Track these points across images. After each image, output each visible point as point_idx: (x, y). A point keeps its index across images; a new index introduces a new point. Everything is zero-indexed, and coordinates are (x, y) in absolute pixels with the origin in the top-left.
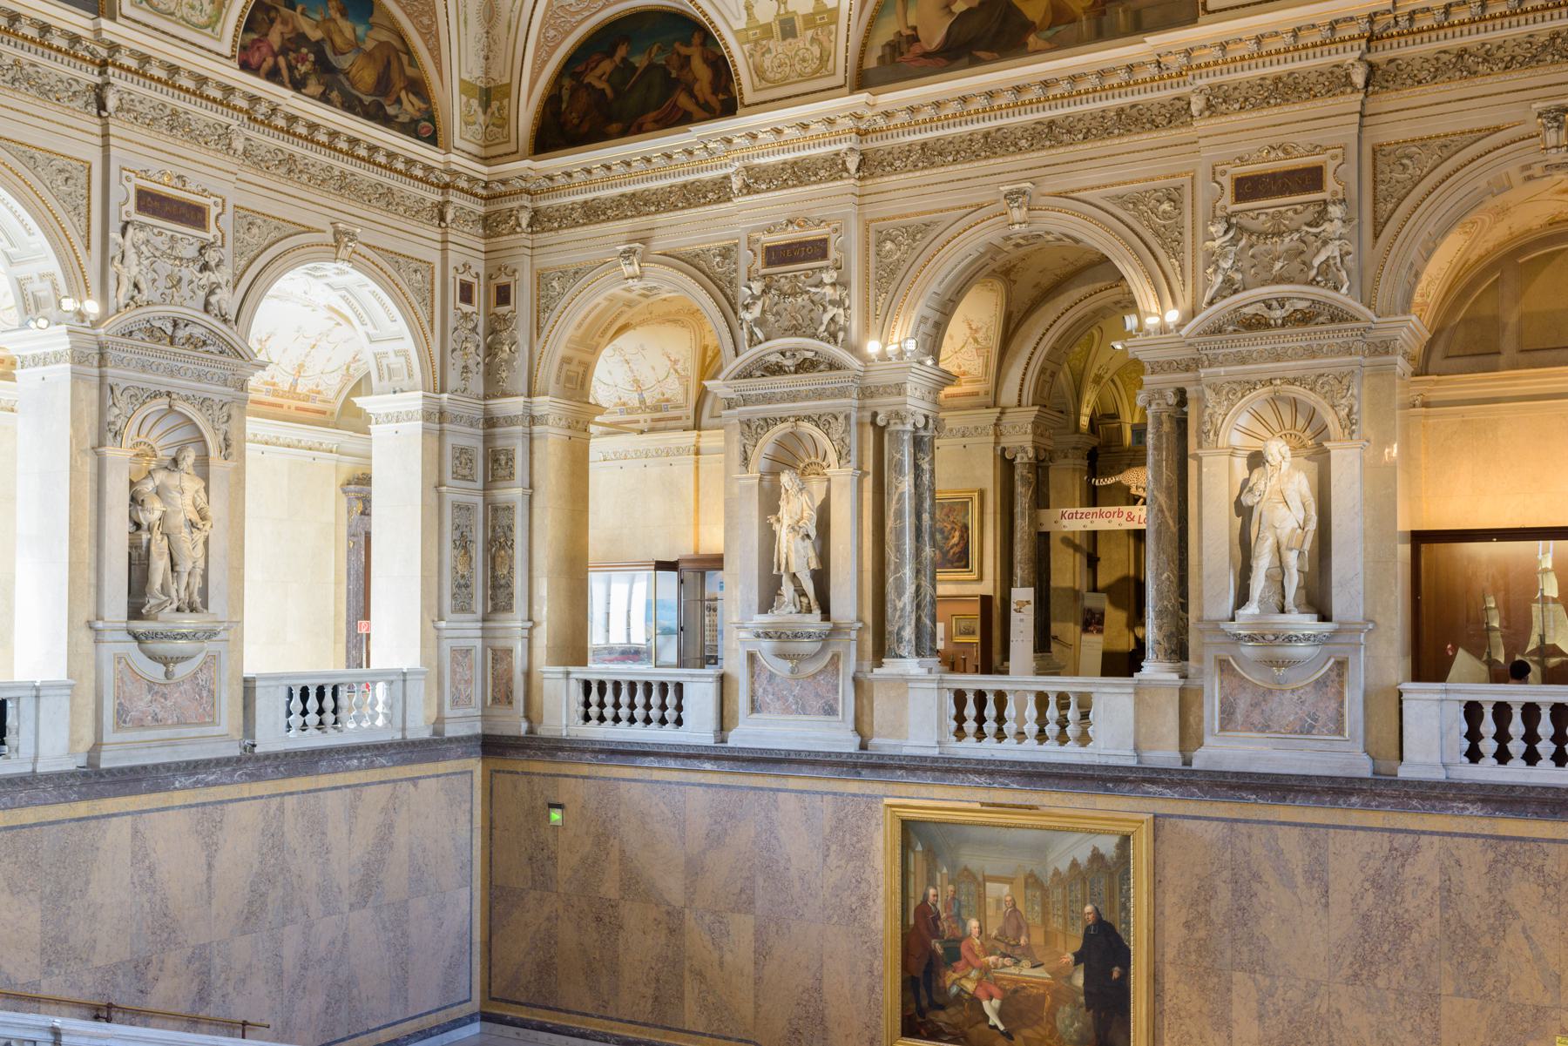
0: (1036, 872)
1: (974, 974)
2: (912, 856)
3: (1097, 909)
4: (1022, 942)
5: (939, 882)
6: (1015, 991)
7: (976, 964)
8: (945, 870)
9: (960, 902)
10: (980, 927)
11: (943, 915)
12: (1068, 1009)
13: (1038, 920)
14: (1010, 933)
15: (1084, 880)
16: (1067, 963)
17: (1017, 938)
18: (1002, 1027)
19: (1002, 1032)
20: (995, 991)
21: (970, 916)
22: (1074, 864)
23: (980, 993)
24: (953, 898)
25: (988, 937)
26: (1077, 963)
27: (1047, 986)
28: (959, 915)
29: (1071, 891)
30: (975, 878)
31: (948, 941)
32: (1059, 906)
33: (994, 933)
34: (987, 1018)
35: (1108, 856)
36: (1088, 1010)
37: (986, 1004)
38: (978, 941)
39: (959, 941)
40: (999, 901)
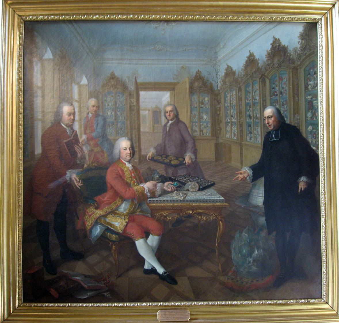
0: (205, 74)
1: (124, 207)
2: (37, 68)
3: (278, 111)
4: (187, 160)
5: (76, 96)
6: (179, 222)
7: (127, 194)
8: (84, 81)
9: (105, 119)
10: (132, 148)
11: (83, 138)
12: (245, 235)
13: (207, 132)
14: (171, 150)
15: (263, 79)
16: (244, 179)
17: (180, 156)
18: (161, 270)
19: (161, 276)
20: (152, 224)
21: (119, 134)
22: (251, 61)
23: (133, 231)
24: (96, 115)
25: (142, 159)
26: (255, 177)
27: (217, 209)
28: (104, 136)
29: (247, 92)
30: (124, 87)
31: (90, 169)
32: (234, 112)
33: (151, 152)
34: (142, 261)
35: (290, 49)
36: (269, 233)
37: (140, 244)
38: (129, 166)
39: (103, 168)
40: (156, 113)
